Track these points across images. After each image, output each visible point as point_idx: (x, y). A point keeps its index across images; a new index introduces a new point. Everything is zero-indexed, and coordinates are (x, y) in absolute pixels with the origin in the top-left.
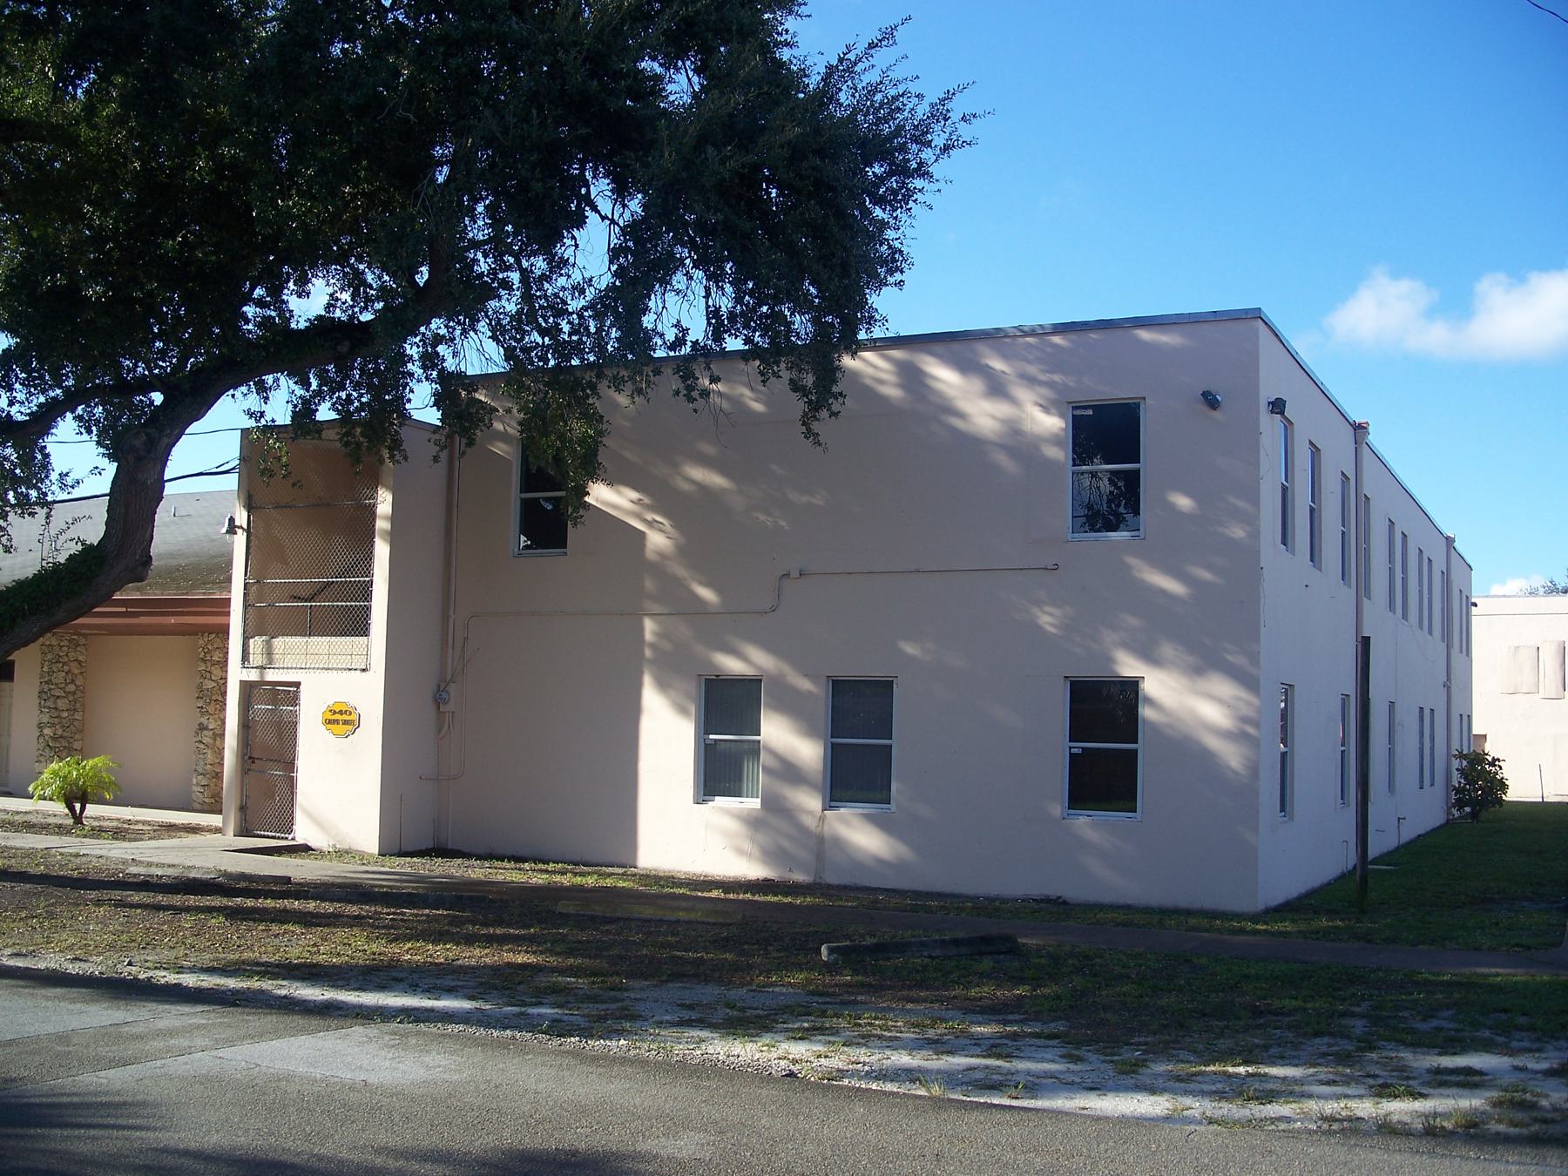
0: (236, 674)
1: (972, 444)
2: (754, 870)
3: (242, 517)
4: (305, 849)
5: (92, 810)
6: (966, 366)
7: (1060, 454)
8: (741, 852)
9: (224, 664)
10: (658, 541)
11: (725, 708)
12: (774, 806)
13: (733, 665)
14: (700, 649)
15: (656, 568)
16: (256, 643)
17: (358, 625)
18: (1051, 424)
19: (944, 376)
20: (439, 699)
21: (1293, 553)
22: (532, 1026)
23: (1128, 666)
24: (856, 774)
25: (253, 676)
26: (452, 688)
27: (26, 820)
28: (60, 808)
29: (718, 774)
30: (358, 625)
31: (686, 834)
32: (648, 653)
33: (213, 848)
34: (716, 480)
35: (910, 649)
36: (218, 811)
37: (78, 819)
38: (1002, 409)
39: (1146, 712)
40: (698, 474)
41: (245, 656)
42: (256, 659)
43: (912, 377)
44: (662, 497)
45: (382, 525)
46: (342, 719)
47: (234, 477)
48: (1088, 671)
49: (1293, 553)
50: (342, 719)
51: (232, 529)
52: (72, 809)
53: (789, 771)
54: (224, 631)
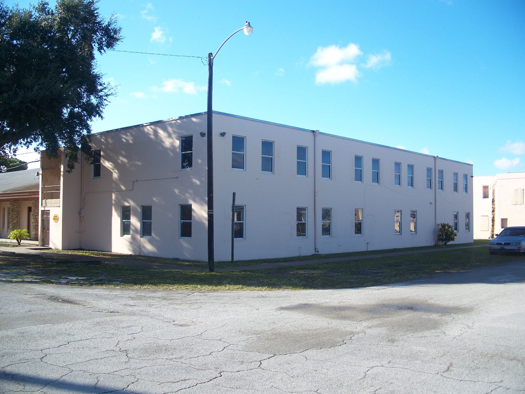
0: (41, 209)
1: (165, 149)
2: (130, 253)
3: (41, 172)
4: (51, 248)
5: (22, 241)
6: (165, 130)
7: (179, 150)
8: (129, 250)
9: (38, 207)
10: (115, 175)
11: (125, 214)
12: (133, 238)
13: (127, 204)
14: (122, 201)
15: (115, 182)
16: (44, 201)
17: (58, 197)
18: (177, 143)
19: (161, 133)
20: (80, 214)
21: (274, 174)
22: (62, 284)
23: (191, 202)
24: (146, 230)
25: (43, 209)
26: (82, 210)
27: (10, 244)
28: (15, 241)
29: (125, 229)
30: (58, 197)
31: (120, 245)
32: (113, 202)
33: (28, 247)
34: (125, 160)
35: (154, 199)
36: (37, 240)
37: (19, 244)
38: (170, 140)
39: (193, 214)
40: (121, 158)
41: (42, 205)
42: (44, 205)
43: (156, 133)
44: (117, 166)
45: (62, 173)
46: (56, 218)
47: (39, 162)
48: (183, 203)
49: (274, 174)
50: (56, 218)
51: (38, 174)
52: (18, 241)
53: (136, 231)
54: (38, 198)
